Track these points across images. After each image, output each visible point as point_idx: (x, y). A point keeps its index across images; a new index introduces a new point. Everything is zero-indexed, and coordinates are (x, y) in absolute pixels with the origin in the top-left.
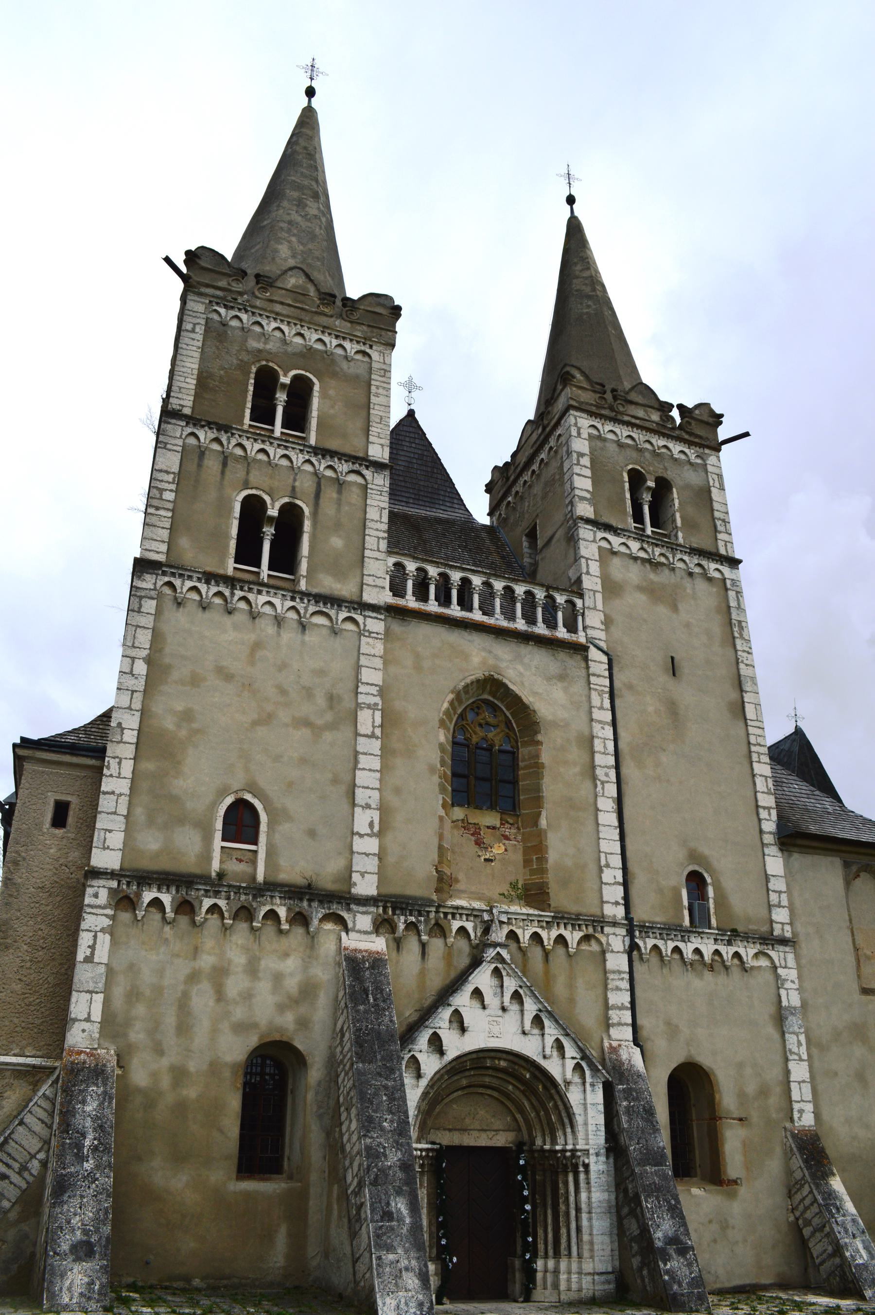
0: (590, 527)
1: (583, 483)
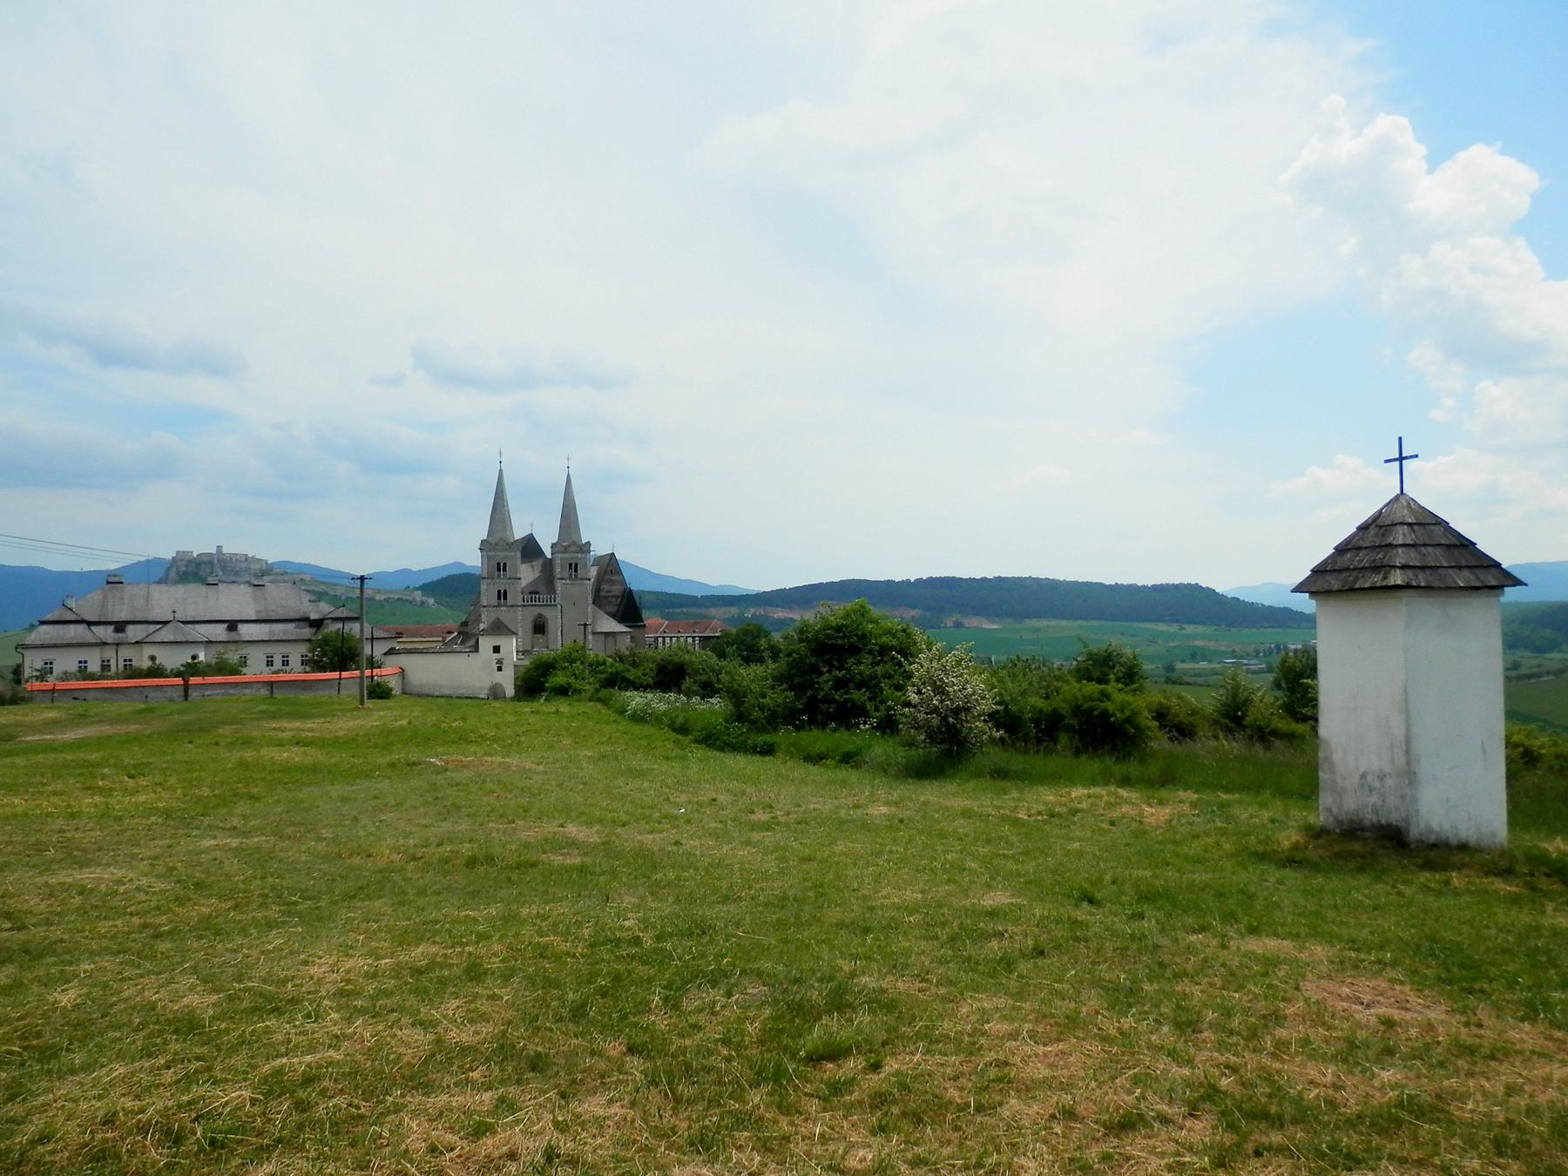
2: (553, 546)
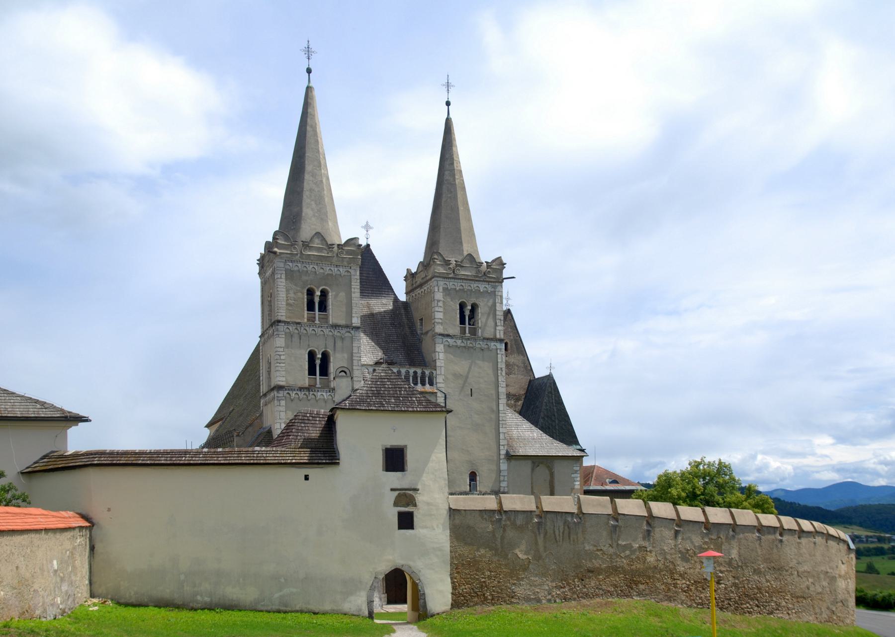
0: (441, 337)
1: (439, 316)
2: (410, 277)
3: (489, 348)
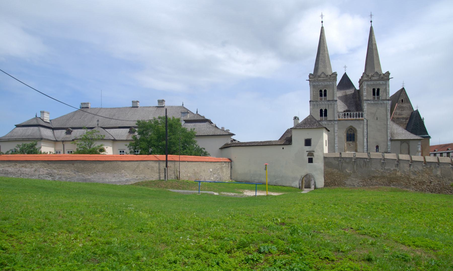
3: (384, 103)
